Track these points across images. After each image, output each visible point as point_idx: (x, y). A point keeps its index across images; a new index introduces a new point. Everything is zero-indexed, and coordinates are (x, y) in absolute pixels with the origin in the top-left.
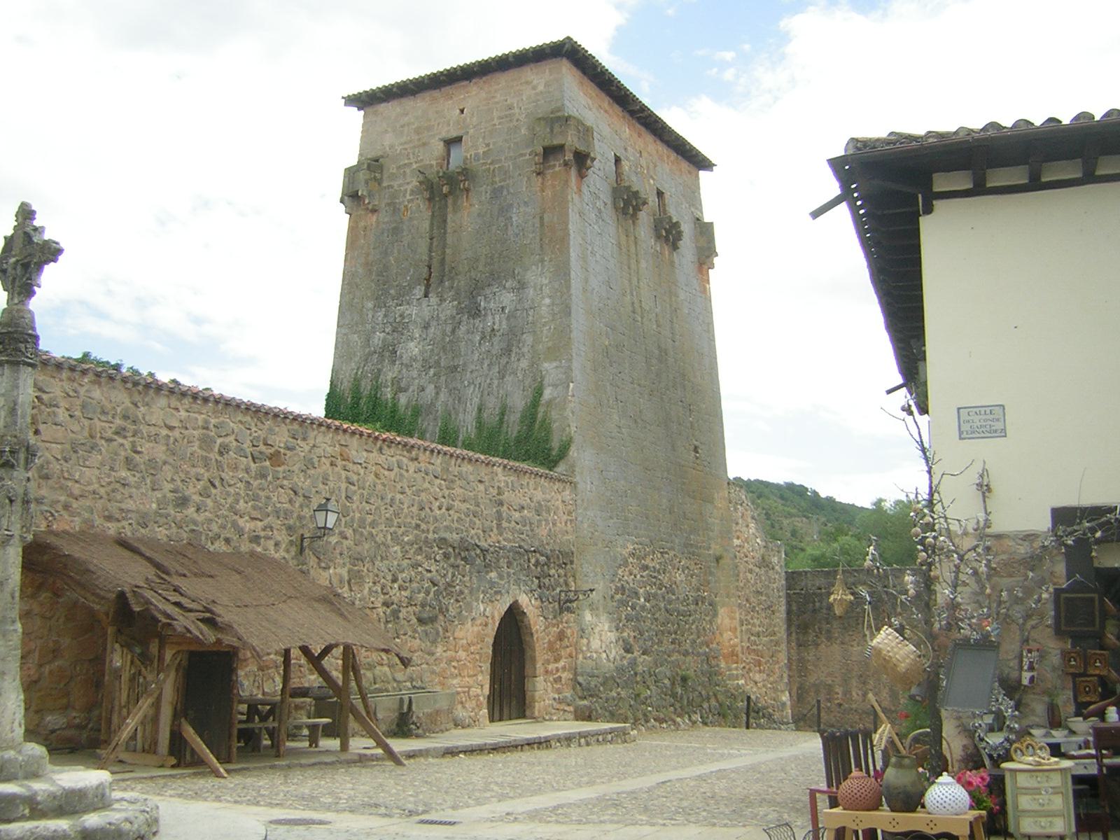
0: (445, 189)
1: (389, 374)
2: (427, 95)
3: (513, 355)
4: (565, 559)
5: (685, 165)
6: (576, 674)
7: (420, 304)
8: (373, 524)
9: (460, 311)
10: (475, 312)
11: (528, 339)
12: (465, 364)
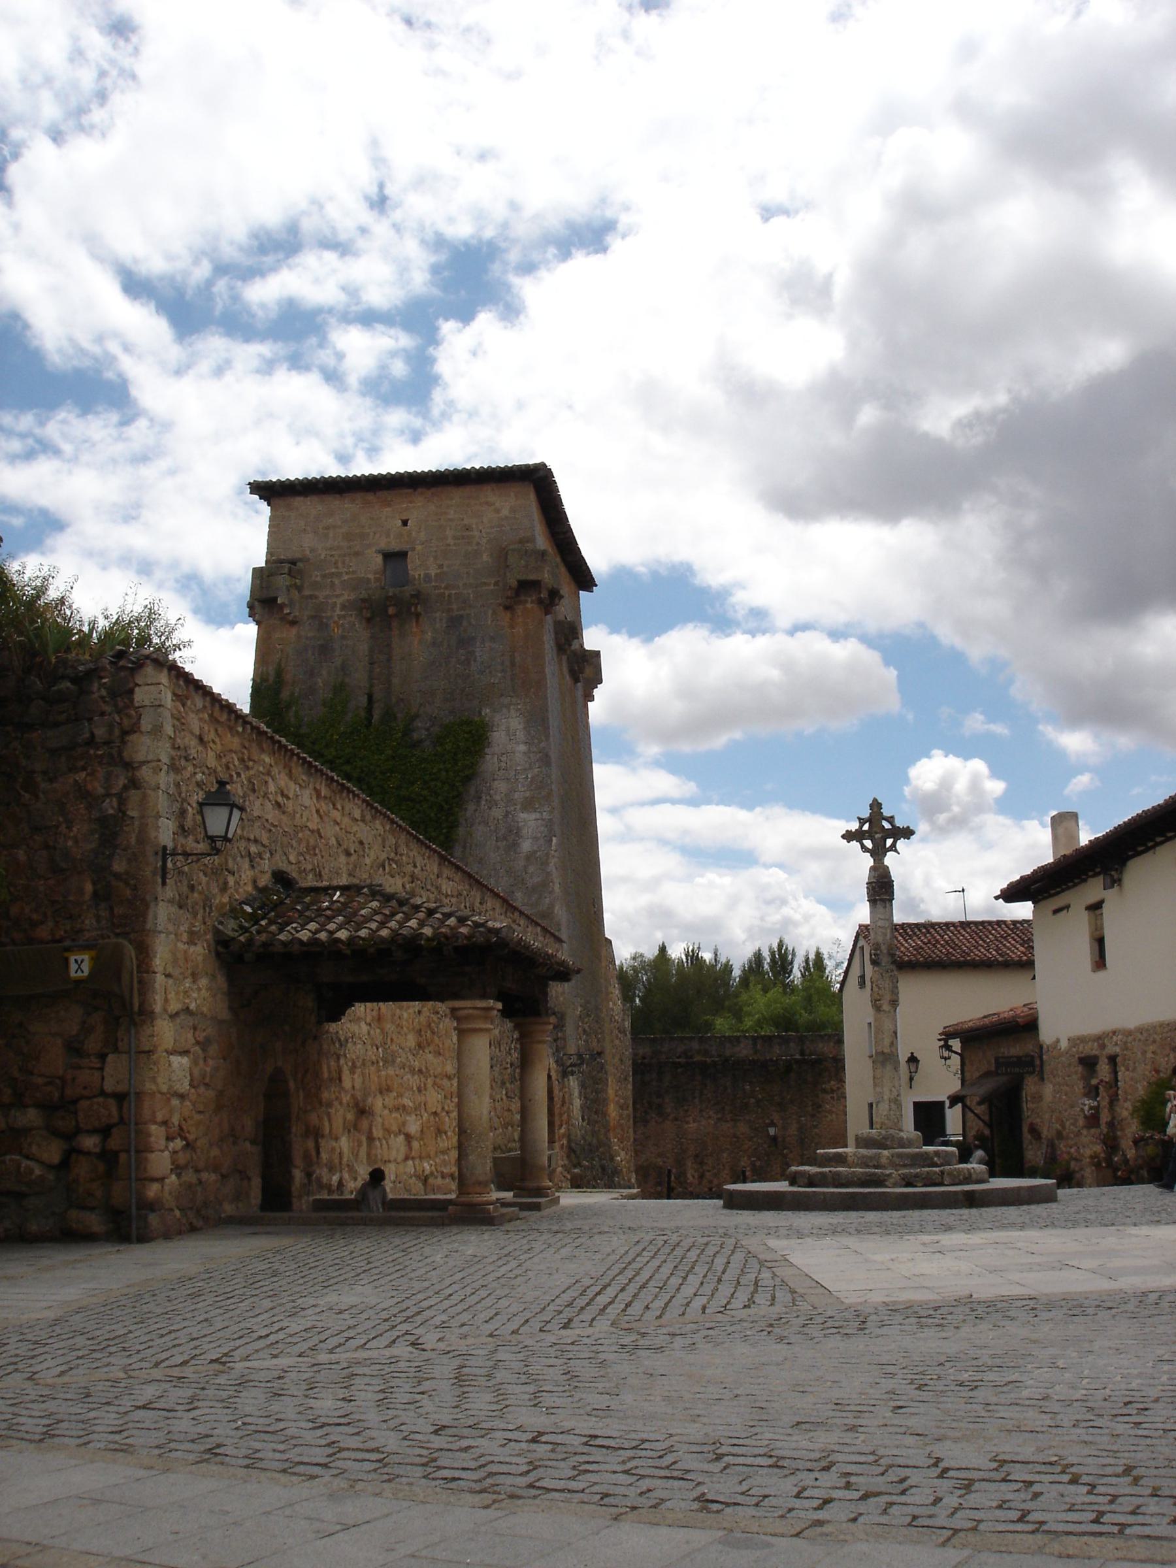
0: (391, 611)
2: (359, 496)
3: (483, 803)
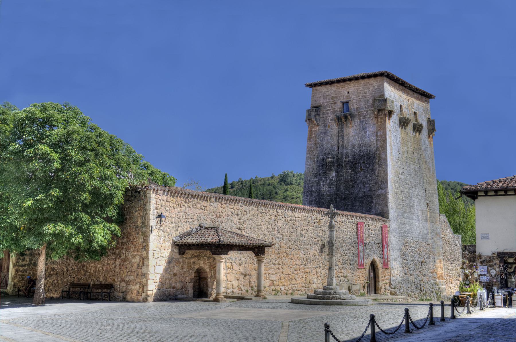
2: (336, 84)
6: (390, 281)
8: (339, 238)
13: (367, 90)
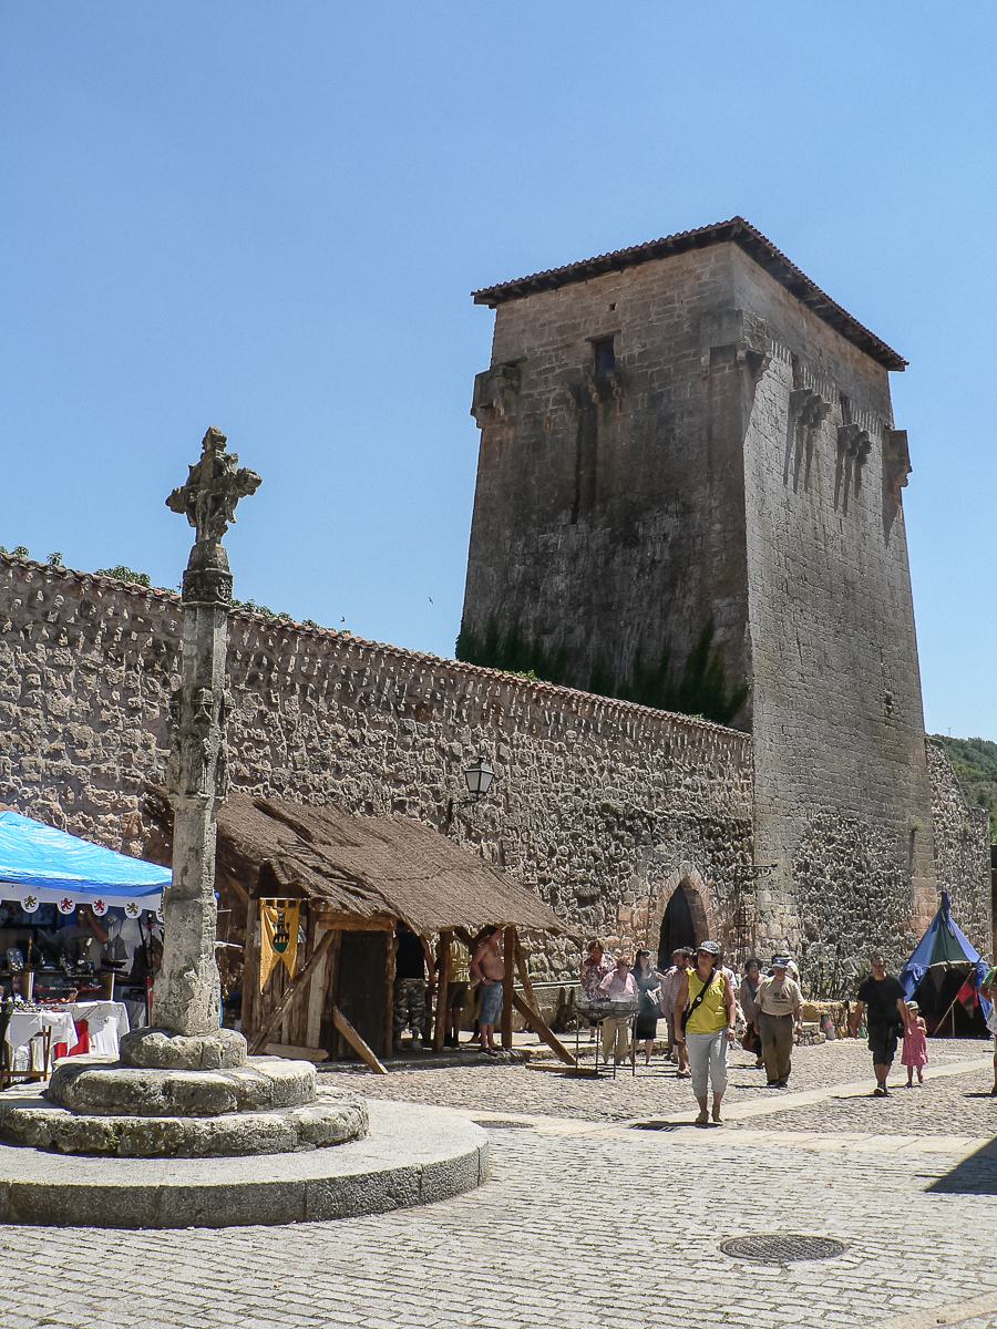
1: (532, 613)
4: (741, 830)
5: (871, 364)
7: (568, 533)
9: (614, 539)
10: (632, 540)
11: (696, 571)
12: (620, 601)
13: (675, 293)
